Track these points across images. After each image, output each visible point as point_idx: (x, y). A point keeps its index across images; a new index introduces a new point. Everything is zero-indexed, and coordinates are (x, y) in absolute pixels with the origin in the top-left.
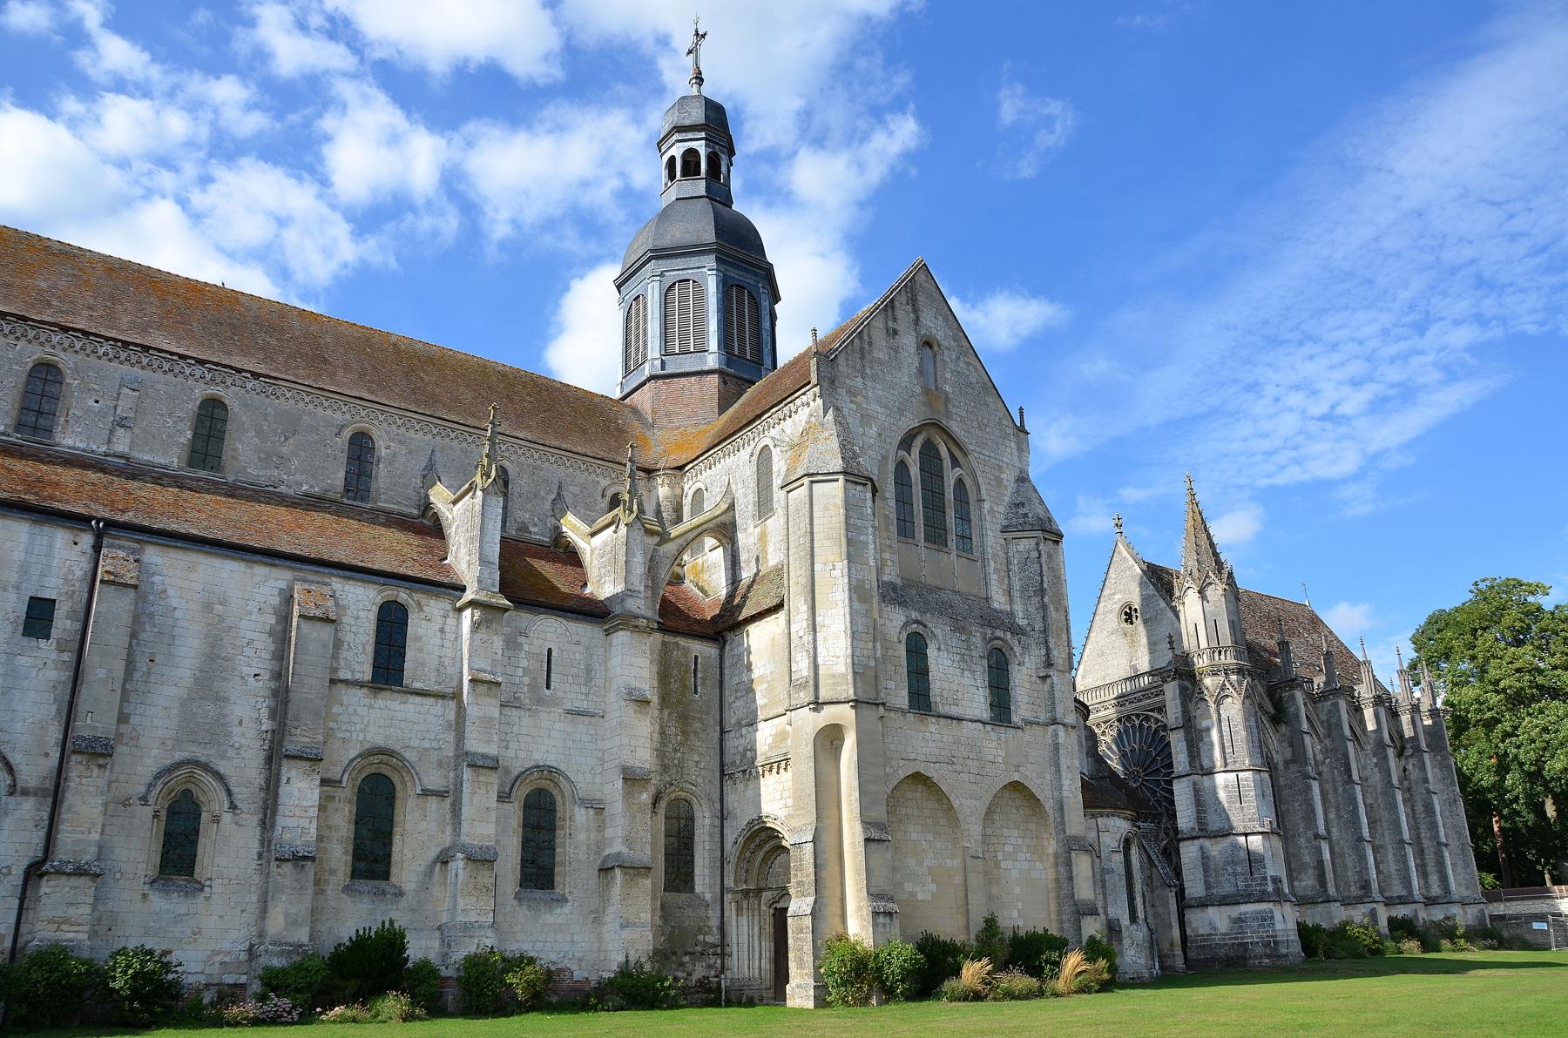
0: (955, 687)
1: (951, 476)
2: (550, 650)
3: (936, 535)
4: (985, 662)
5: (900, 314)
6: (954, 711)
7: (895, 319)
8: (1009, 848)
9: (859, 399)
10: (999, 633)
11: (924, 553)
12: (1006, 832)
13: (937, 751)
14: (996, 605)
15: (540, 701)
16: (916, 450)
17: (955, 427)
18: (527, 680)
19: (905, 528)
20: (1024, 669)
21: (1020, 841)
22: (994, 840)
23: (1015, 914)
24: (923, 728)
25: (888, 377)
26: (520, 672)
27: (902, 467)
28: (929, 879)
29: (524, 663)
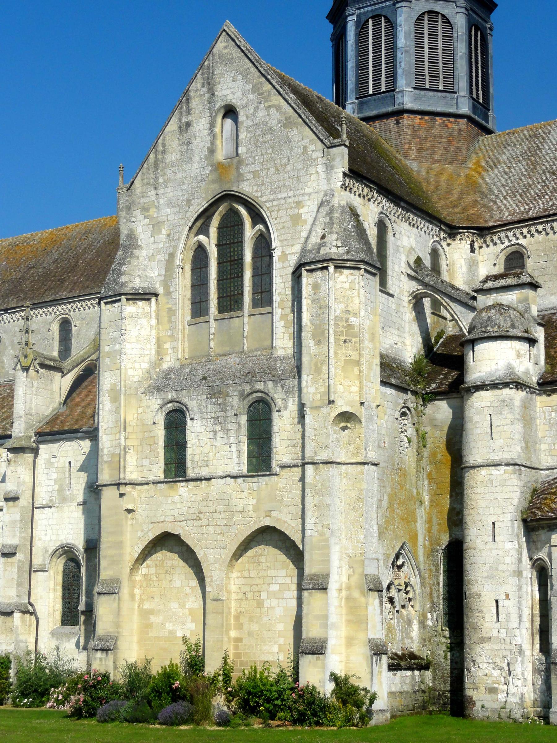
0: (206, 450)
1: (250, 232)
2: (70, 462)
3: (230, 302)
4: (244, 419)
5: (195, 103)
6: (205, 472)
7: (189, 112)
8: (275, 588)
9: (152, 212)
10: (260, 386)
11: (213, 324)
12: (272, 573)
13: (185, 511)
14: (280, 353)
15: (64, 499)
16: (213, 230)
17: (246, 188)
18: (57, 487)
19: (199, 307)
20: (286, 414)
21: (288, 580)
22: (258, 581)
23: (276, 649)
24: (172, 493)
25: (179, 175)
26: (53, 482)
27: (201, 250)
28: (189, 618)
29: (55, 476)
